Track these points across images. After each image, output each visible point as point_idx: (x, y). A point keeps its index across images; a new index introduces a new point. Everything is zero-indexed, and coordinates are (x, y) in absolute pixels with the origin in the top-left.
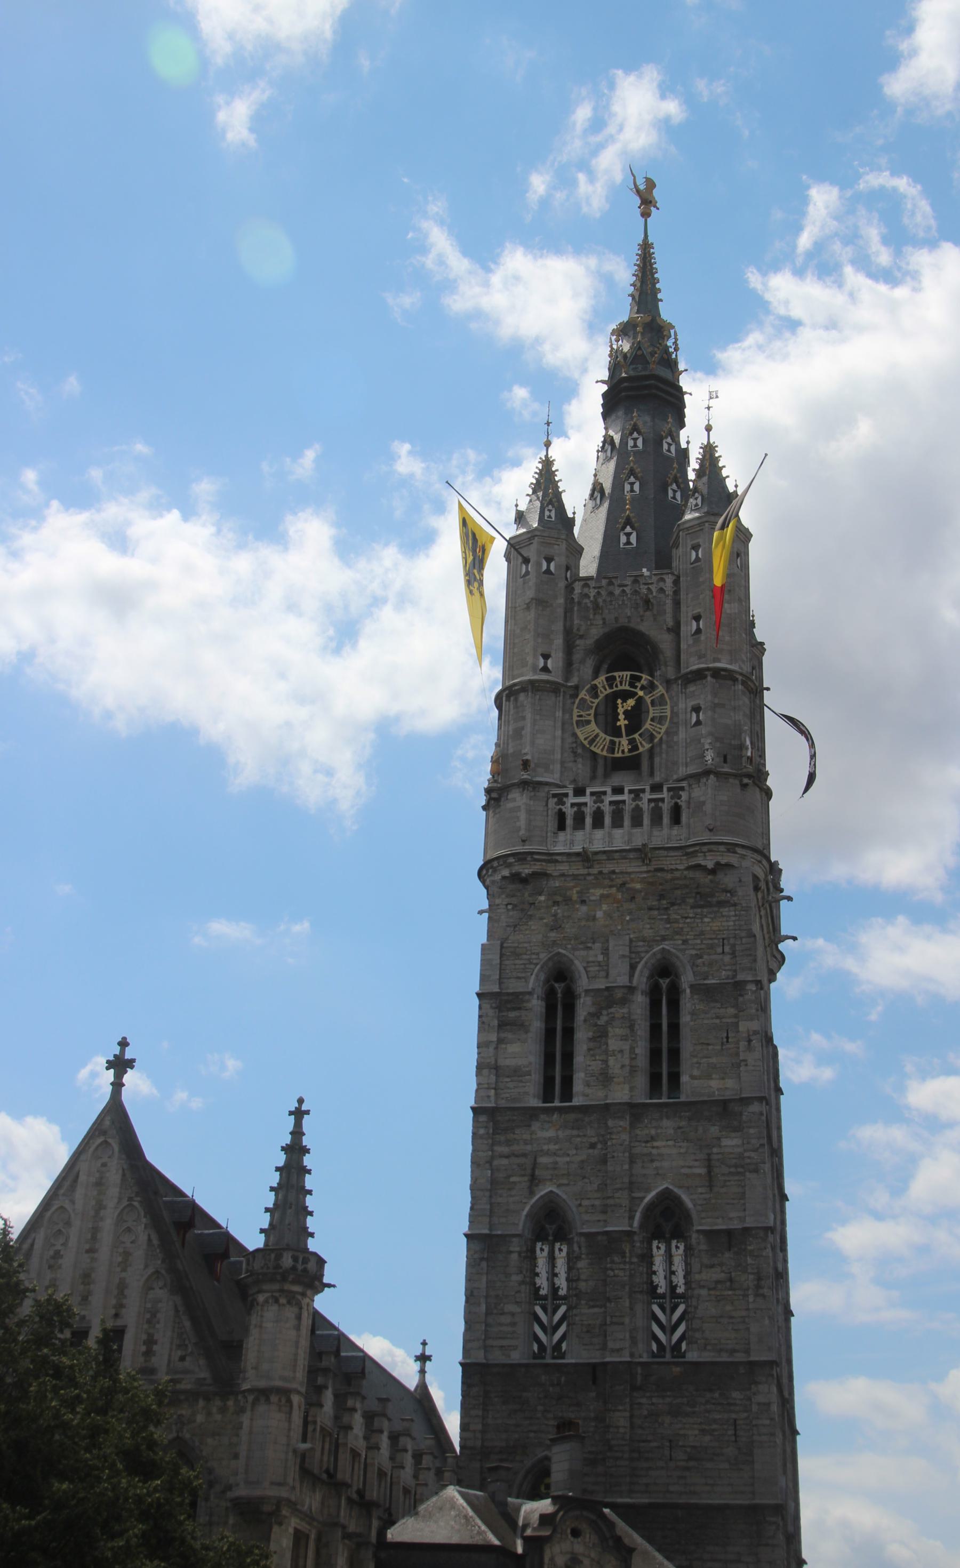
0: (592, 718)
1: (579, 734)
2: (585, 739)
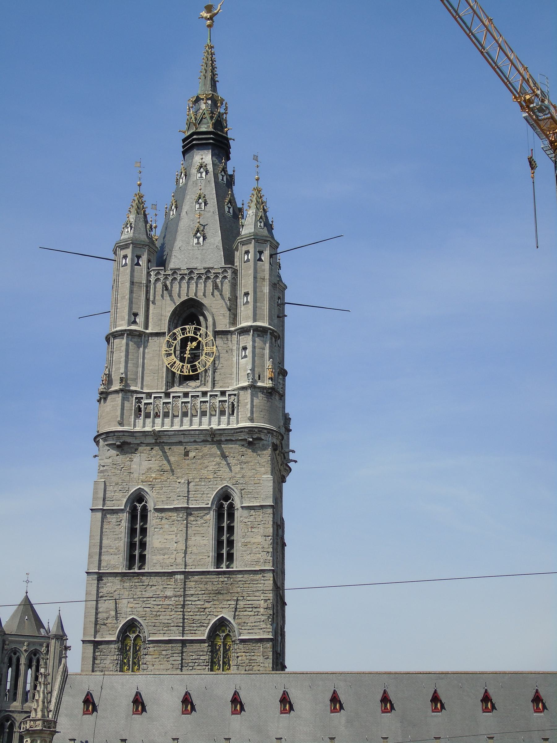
0: (172, 352)
1: (165, 360)
2: (168, 364)
